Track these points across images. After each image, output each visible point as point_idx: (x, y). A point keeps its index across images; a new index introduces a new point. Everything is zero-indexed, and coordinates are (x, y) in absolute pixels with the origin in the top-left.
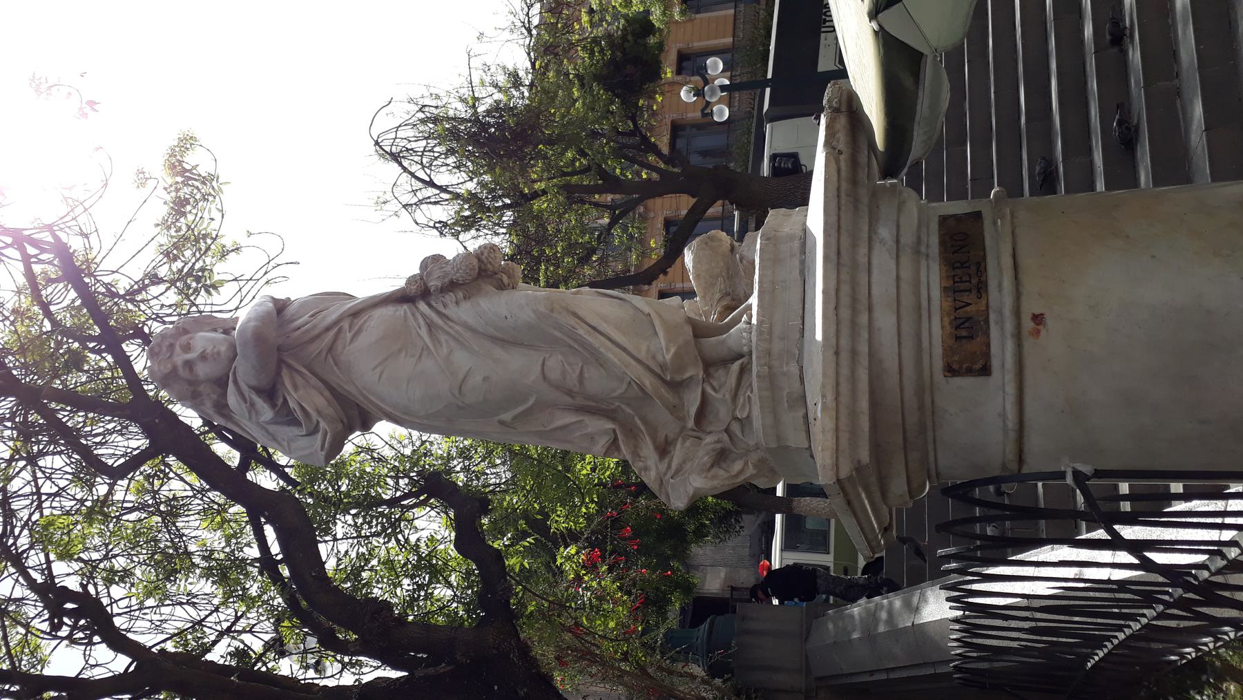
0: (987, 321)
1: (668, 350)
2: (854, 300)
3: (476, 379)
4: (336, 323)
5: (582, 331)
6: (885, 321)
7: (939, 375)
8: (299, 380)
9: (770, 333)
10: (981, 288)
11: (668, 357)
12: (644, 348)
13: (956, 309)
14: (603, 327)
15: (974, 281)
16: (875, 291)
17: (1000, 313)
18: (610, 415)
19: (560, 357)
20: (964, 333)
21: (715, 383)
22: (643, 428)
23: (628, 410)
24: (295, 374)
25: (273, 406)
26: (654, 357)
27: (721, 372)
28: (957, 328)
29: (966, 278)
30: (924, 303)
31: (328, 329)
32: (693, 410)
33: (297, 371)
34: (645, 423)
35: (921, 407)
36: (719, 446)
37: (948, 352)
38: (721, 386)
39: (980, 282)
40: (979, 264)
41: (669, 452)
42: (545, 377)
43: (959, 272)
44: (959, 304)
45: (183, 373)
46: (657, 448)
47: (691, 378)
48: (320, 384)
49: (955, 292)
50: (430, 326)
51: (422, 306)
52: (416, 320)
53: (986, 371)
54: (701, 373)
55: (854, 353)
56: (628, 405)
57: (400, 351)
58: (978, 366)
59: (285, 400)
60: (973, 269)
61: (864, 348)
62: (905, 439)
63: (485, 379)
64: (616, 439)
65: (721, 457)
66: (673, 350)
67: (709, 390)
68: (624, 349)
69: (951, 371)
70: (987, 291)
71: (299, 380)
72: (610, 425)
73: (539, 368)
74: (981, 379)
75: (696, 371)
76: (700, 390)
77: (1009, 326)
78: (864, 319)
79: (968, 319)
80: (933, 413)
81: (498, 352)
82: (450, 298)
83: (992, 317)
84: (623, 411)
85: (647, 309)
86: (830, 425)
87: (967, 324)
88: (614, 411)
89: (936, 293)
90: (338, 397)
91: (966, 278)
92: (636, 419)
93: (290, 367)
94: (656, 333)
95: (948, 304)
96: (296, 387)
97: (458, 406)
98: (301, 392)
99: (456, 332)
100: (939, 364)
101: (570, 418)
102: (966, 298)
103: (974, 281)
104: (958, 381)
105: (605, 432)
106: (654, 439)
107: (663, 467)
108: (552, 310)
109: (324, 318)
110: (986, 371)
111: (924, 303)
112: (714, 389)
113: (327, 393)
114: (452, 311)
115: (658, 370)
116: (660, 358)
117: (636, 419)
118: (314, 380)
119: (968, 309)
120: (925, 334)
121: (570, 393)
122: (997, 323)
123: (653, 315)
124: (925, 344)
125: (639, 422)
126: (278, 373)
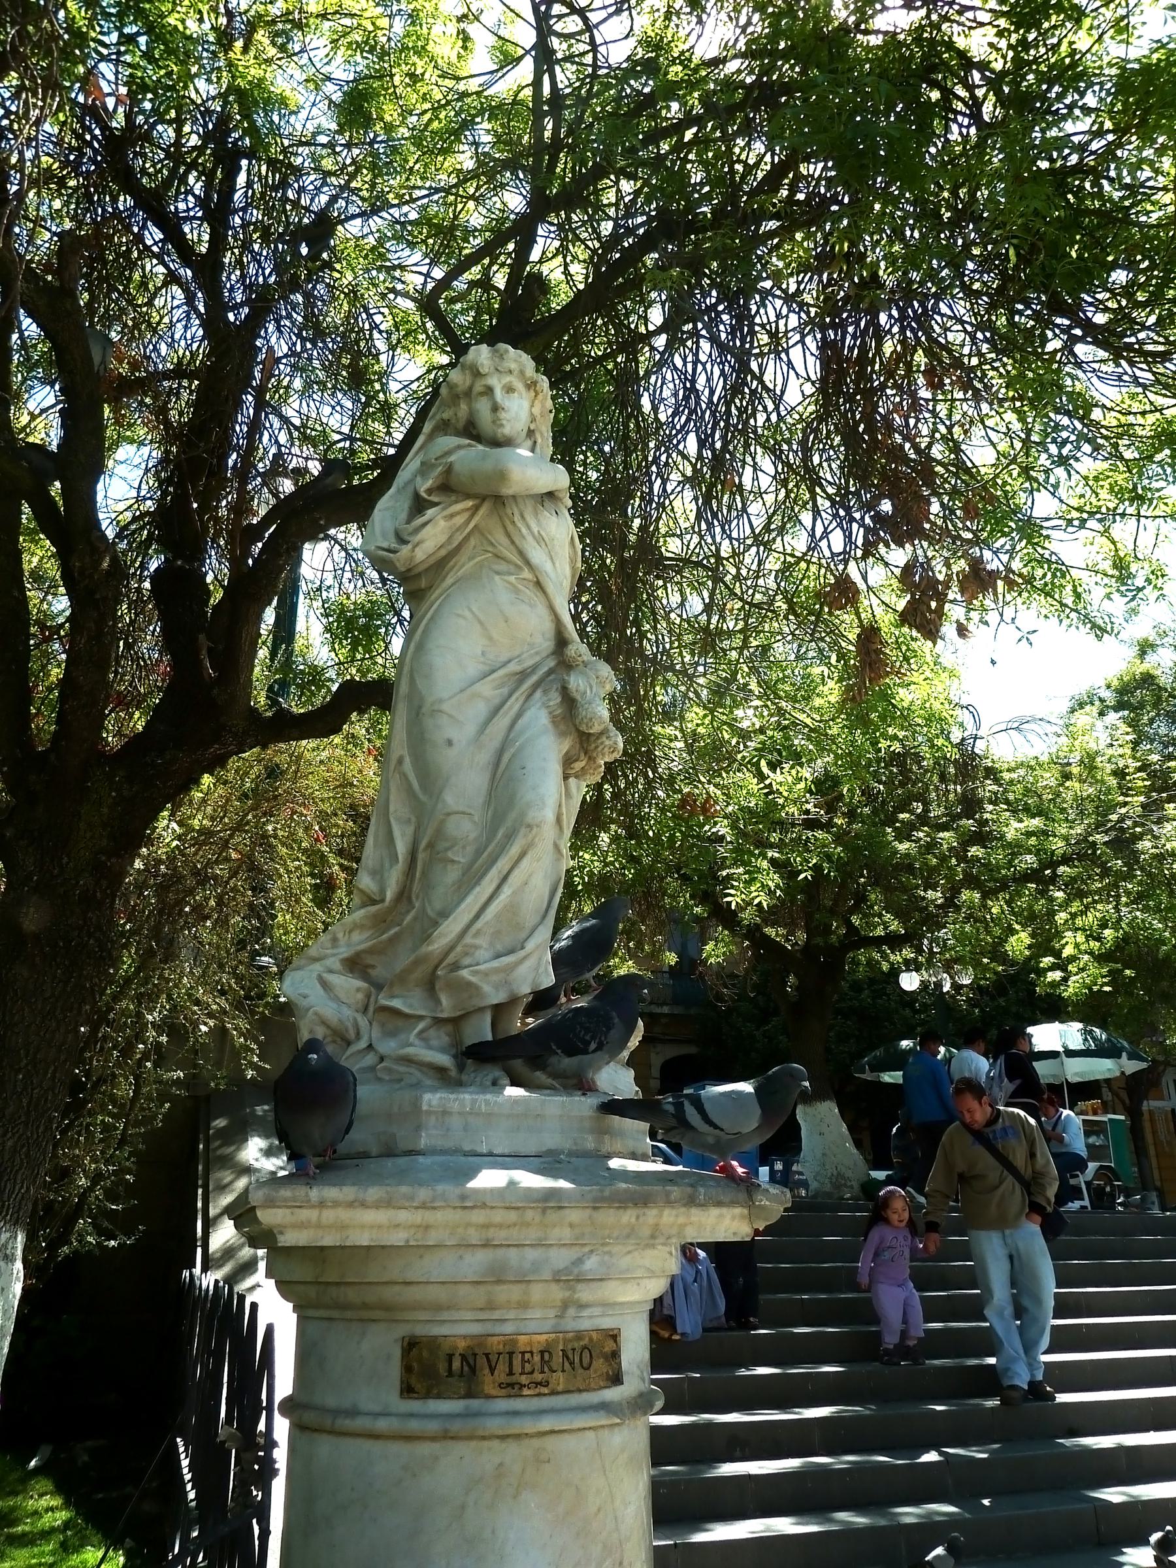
0: (469, 1395)
1: (476, 973)
3: (452, 732)
4: (528, 563)
5: (503, 864)
7: (403, 1330)
8: (459, 520)
11: (465, 973)
12: (477, 941)
13: (487, 1355)
14: (507, 891)
16: (513, 1253)
18: (404, 895)
19: (472, 836)
20: (456, 1364)
22: (385, 936)
23: (409, 918)
24: (466, 515)
25: (430, 491)
26: (467, 954)
27: (446, 1039)
28: (463, 1357)
29: (528, 1367)
30: (496, 1315)
31: (521, 554)
32: (396, 1003)
33: (472, 516)
34: (391, 940)
35: (365, 1306)
36: (352, 1034)
37: (433, 1343)
38: (425, 1040)
39: (522, 1386)
40: (546, 1384)
41: (351, 971)
42: (449, 814)
43: (537, 1358)
44: (493, 1358)
45: (478, 388)
46: (358, 955)
47: (438, 1002)
48: (456, 543)
50: (523, 675)
51: (551, 663)
53: (407, 1391)
54: (445, 1015)
56: (415, 919)
58: (413, 1382)
59: (436, 504)
60: (538, 1377)
62: (328, 1283)
63: (450, 743)
64: (374, 902)
66: (473, 979)
67: (421, 1026)
68: (477, 916)
69: (411, 1345)
71: (459, 520)
72: (389, 895)
73: (461, 809)
74: (397, 1384)
75: (447, 1006)
76: (423, 1013)
79: (473, 1370)
80: (361, 1320)
81: (484, 757)
82: (555, 698)
83: (475, 1404)
84: (408, 912)
85: (530, 945)
87: (466, 1368)
88: (409, 899)
89: (508, 1328)
90: (440, 565)
91: (528, 1367)
92: (397, 929)
93: (476, 509)
94: (498, 956)
96: (452, 516)
97: (420, 707)
98: (442, 523)
99: (511, 708)
100: (420, 1330)
101: (401, 847)
102: (502, 1367)
103: (524, 1379)
104: (397, 1353)
105: (383, 891)
106: (370, 951)
108: (529, 826)
110: (407, 1391)
111: (496, 1315)
112: (422, 1032)
113: (443, 552)
115: (451, 958)
116: (467, 961)
117: (397, 929)
118: (459, 538)
119: (487, 1371)
122: (467, 1408)
123: (522, 953)
124: (445, 1316)
125: (392, 932)
126: (468, 496)
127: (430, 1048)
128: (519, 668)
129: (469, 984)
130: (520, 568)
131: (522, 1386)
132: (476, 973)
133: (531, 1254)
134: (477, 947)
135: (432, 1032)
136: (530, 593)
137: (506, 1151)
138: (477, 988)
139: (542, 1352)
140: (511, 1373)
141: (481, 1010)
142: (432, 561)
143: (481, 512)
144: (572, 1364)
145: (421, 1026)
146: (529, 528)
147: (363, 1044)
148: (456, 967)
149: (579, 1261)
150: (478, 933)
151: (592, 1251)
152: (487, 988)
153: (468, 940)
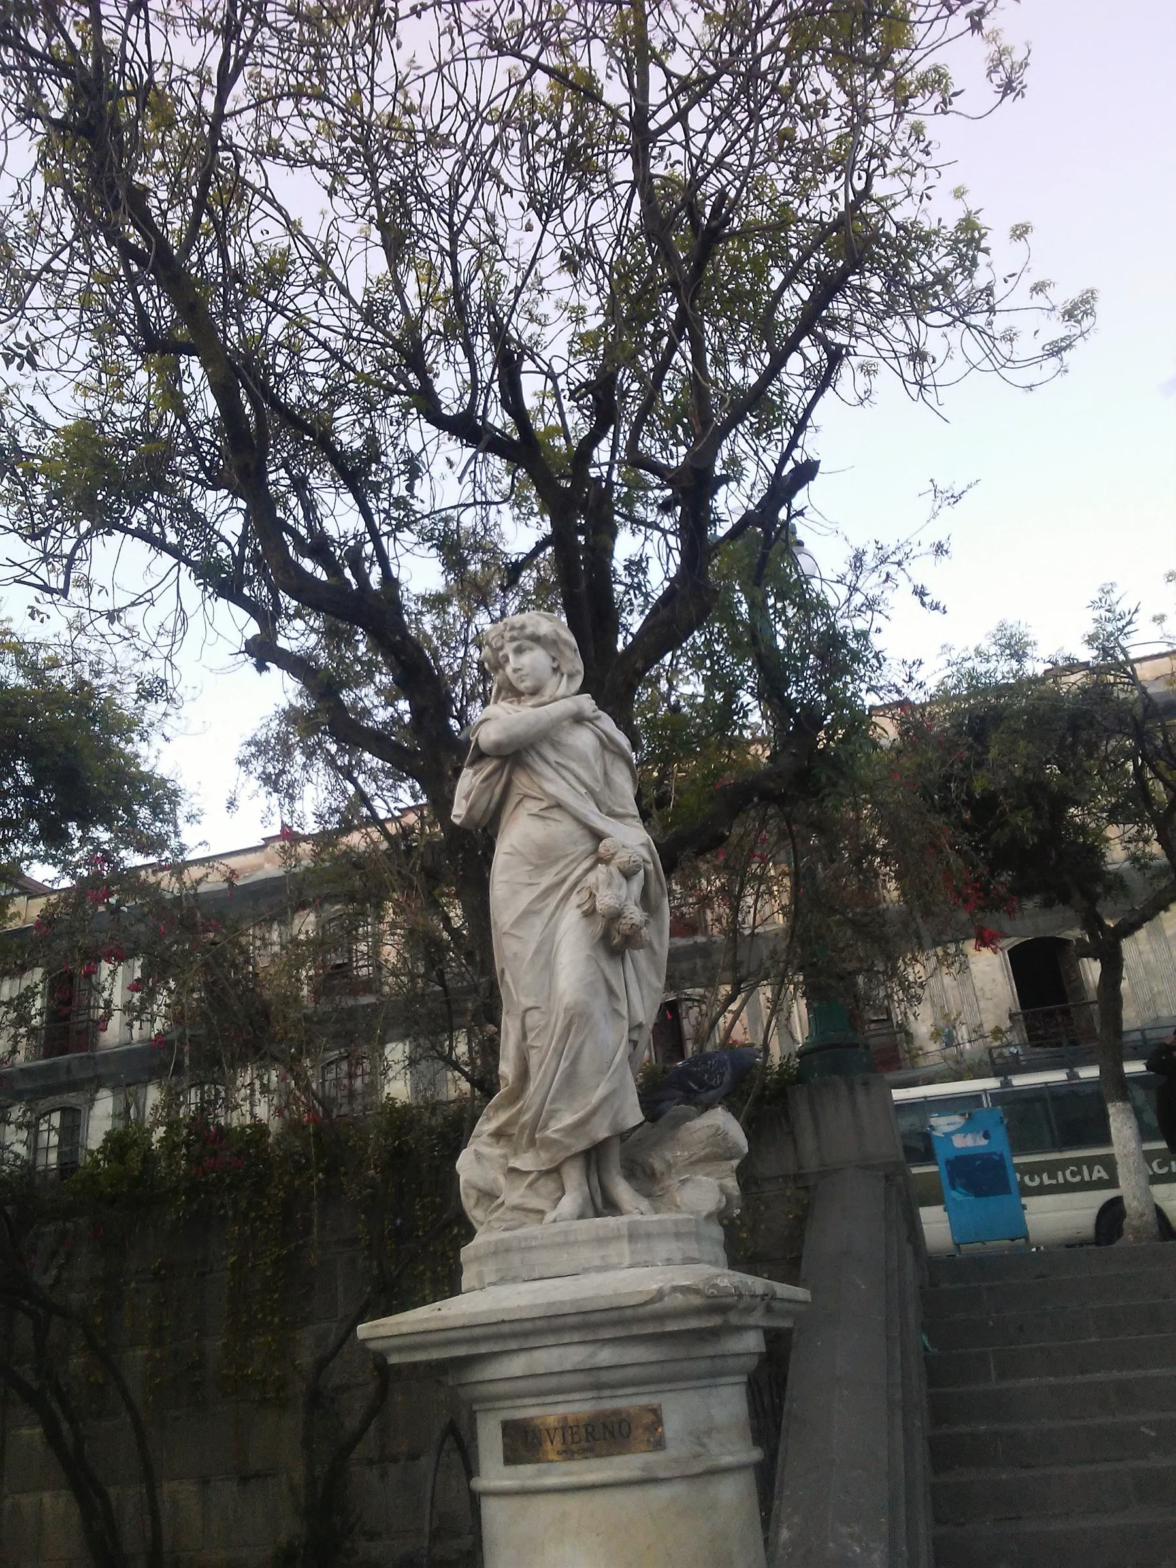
0: (538, 1461)
2: (526, 1335)
6: (516, 1365)
9: (530, 1248)
10: (568, 1454)
11: (549, 1133)
15: (574, 1447)
17: (546, 1473)
21: (541, 1182)
29: (576, 1438)
43: (583, 1430)
49: (563, 1428)
51: (586, 864)
52: (566, 866)
55: (475, 1340)
57: (531, 864)
60: (585, 1444)
61: (483, 1349)
65: (488, 1196)
66: (555, 1136)
67: (531, 1177)
70: (564, 1460)
77: (531, 1483)
78: (513, 1345)
82: (585, 895)
83: (543, 1466)
86: (405, 1329)
89: (561, 1410)
91: (576, 1438)
95: (552, 1421)
102: (558, 1439)
103: (574, 1447)
107: (484, 1138)
109: (550, 780)
113: (492, 805)
114: (575, 899)
118: (498, 790)
120: (527, 1401)
121: (524, 1036)
124: (518, 1402)
127: (538, 1195)
131: (573, 1453)
133: (556, 1352)
136: (556, 814)
139: (586, 1426)
140: (564, 1443)
142: (489, 815)
144: (612, 1434)
145: (531, 1177)
146: (548, 763)
147: (500, 1200)
148: (545, 1127)
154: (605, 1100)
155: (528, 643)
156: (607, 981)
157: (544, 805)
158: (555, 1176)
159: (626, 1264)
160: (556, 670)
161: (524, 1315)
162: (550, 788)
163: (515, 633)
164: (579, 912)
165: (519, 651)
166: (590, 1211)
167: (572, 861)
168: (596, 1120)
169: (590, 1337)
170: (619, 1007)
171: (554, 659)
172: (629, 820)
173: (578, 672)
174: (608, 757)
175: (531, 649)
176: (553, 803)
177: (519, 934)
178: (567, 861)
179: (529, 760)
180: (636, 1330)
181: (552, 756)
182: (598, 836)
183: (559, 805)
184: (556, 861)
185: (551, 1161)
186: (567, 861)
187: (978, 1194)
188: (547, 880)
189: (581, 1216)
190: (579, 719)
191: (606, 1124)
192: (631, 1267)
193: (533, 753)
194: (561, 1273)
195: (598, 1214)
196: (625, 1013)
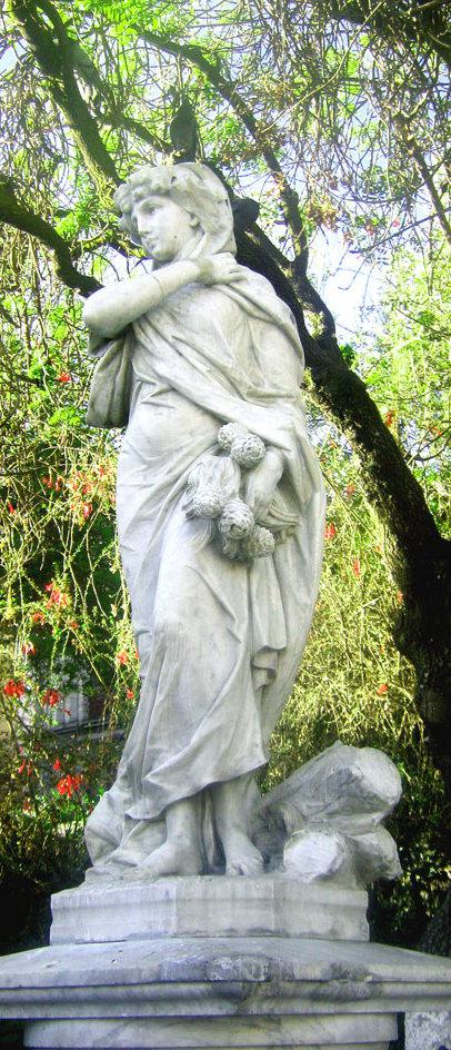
4: (161, 378)
12: (157, 746)
14: (160, 698)
16: (67, 1025)
31: (154, 371)
52: (180, 462)
57: (144, 462)
112: (136, 834)
118: (119, 378)
128: (169, 478)
129: (155, 787)
130: (154, 384)
132: (156, 775)
133: (80, 1026)
134: (158, 752)
135: (148, 833)
136: (170, 399)
137: (103, 938)
138: (161, 788)
141: (171, 806)
143: (125, 350)
149: (115, 1033)
150: (153, 740)
151: (126, 1025)
152: (166, 786)
153: (148, 747)
154: (206, 739)
155: (157, 200)
156: (215, 597)
157: (157, 390)
158: (161, 825)
159: (171, 933)
160: (197, 228)
161: (36, 983)
162: (162, 369)
163: (139, 190)
164: (183, 514)
165: (149, 210)
166: (192, 865)
167: (188, 455)
168: (199, 762)
169: (109, 1014)
170: (235, 631)
171: (193, 216)
172: (280, 401)
173: (222, 228)
174: (252, 323)
175: (161, 207)
176: (165, 386)
177: (131, 546)
178: (180, 455)
179: (141, 337)
180: (148, 1011)
181: (169, 329)
182: (221, 421)
183: (173, 389)
184: (170, 454)
185: (155, 807)
186: (180, 455)
187: (84, 880)
188: (160, 478)
189: (174, 872)
190: (206, 283)
191: (211, 766)
192: (175, 936)
193: (150, 331)
194: (114, 937)
195: (205, 870)
196: (242, 636)
